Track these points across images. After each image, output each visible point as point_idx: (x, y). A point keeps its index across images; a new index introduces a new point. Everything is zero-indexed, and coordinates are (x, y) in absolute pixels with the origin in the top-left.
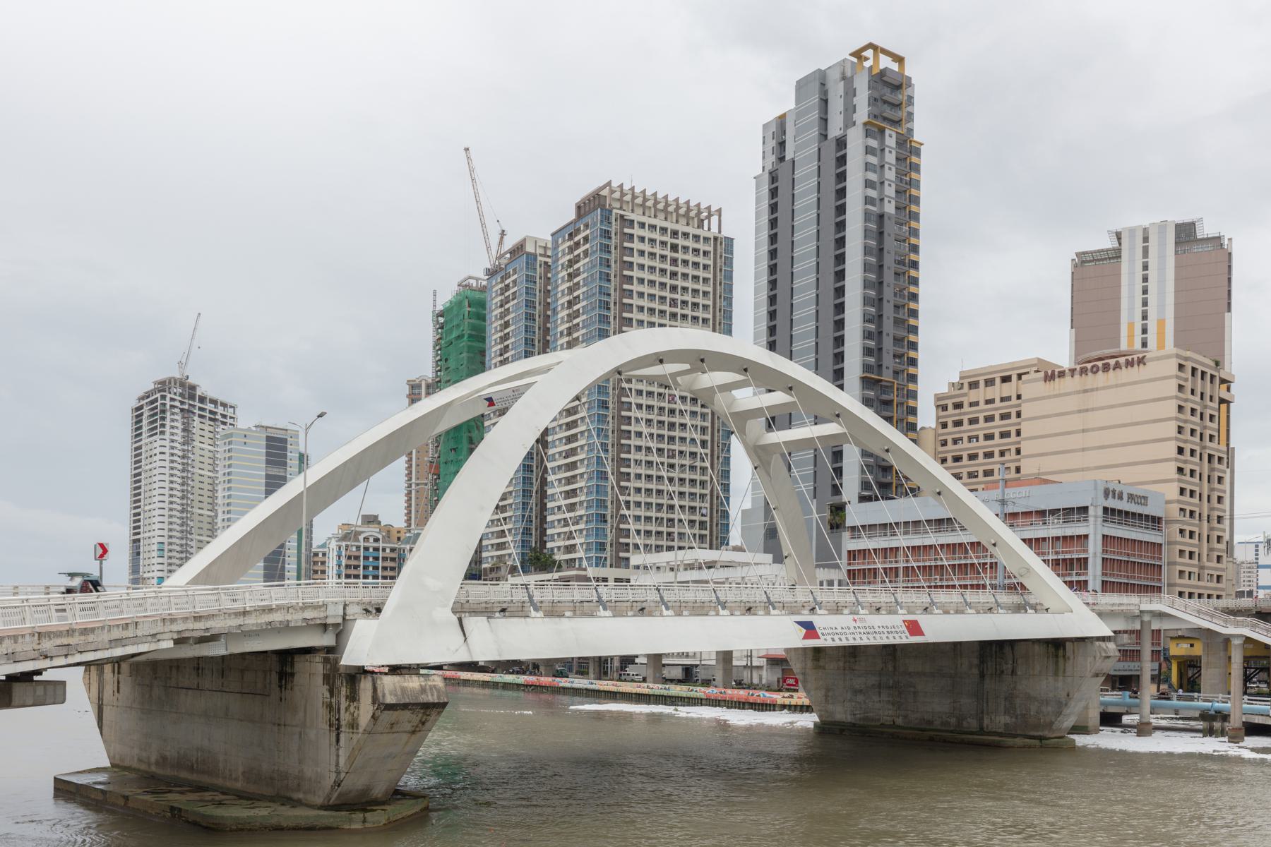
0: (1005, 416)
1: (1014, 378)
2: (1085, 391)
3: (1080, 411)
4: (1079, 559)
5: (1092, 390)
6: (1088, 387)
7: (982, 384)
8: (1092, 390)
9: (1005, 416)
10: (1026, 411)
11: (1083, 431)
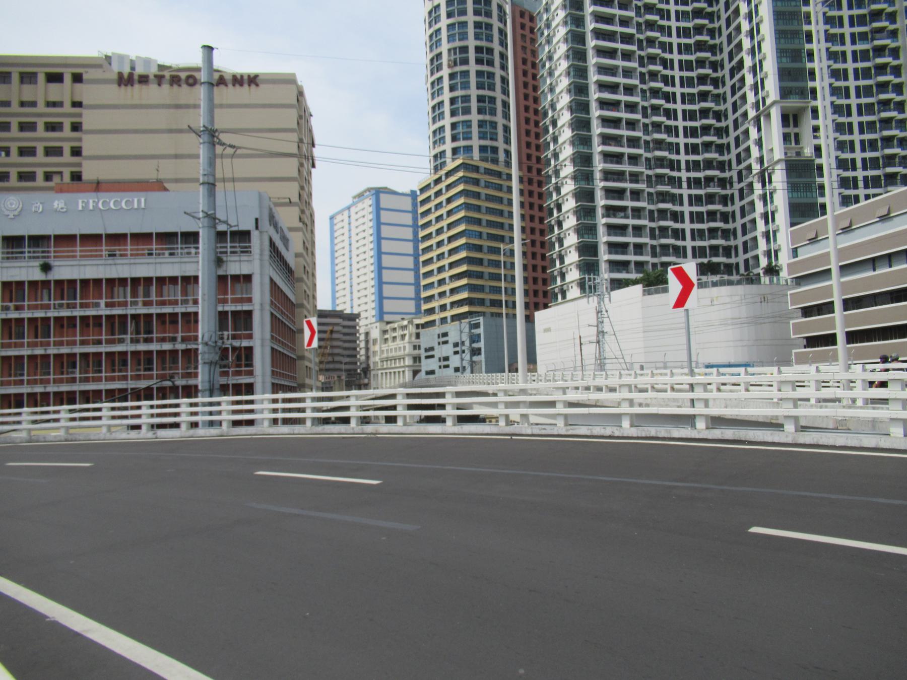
0: (52, 127)
1: (68, 78)
2: (178, 107)
3: (171, 131)
4: (185, 315)
5: (187, 106)
6: (182, 102)
7: (15, 78)
8: (187, 106)
9: (52, 127)
10: (89, 119)
11: (176, 157)
